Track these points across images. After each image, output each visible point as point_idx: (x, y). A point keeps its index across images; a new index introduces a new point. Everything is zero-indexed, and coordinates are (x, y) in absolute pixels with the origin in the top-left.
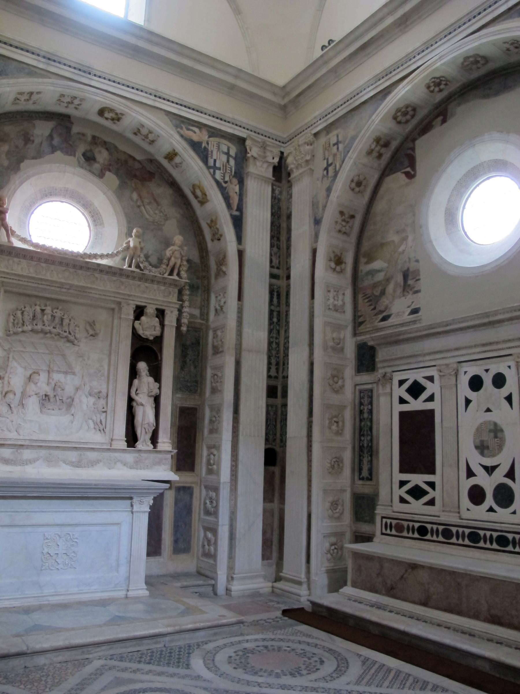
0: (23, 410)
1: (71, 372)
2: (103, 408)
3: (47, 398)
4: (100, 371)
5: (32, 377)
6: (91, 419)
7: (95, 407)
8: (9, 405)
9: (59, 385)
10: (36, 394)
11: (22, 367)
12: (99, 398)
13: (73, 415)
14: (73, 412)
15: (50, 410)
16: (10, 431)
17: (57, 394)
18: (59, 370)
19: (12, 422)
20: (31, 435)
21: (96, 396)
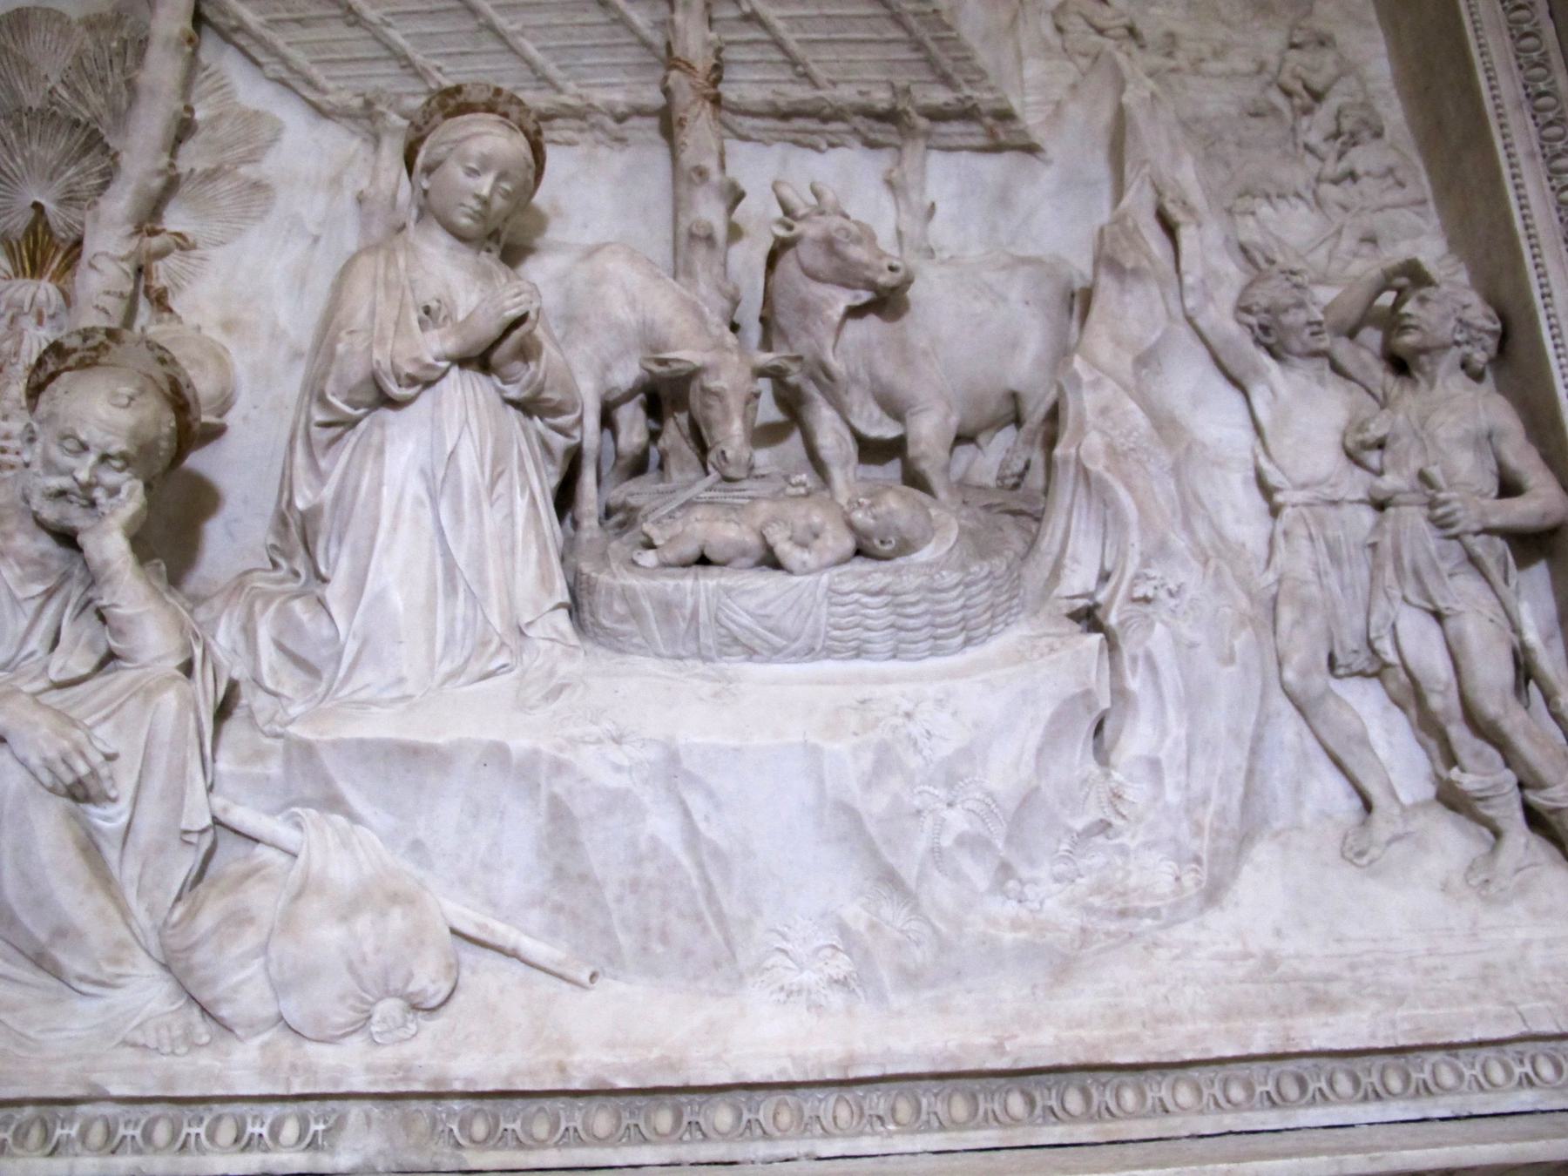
0: (298, 606)
1: (968, 114)
2: (1509, 487)
3: (674, 433)
4: (1317, 96)
5: (420, 160)
6: (1378, 671)
7: (1389, 482)
8: (67, 538)
9: (829, 245)
10: (480, 360)
11: (321, 112)
12: (1400, 365)
13: (1089, 618)
14: (1079, 580)
15: (709, 582)
16: (41, 960)
17: (823, 375)
18: (800, 93)
19: (80, 793)
20: (417, 1007)
21: (1343, 350)
